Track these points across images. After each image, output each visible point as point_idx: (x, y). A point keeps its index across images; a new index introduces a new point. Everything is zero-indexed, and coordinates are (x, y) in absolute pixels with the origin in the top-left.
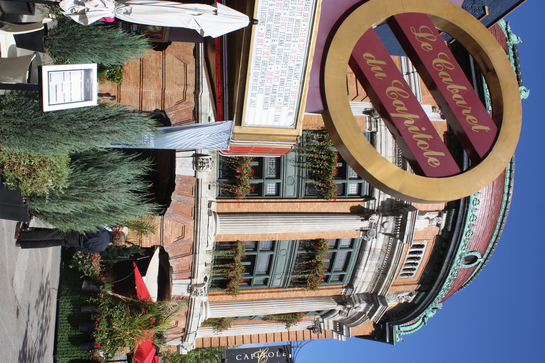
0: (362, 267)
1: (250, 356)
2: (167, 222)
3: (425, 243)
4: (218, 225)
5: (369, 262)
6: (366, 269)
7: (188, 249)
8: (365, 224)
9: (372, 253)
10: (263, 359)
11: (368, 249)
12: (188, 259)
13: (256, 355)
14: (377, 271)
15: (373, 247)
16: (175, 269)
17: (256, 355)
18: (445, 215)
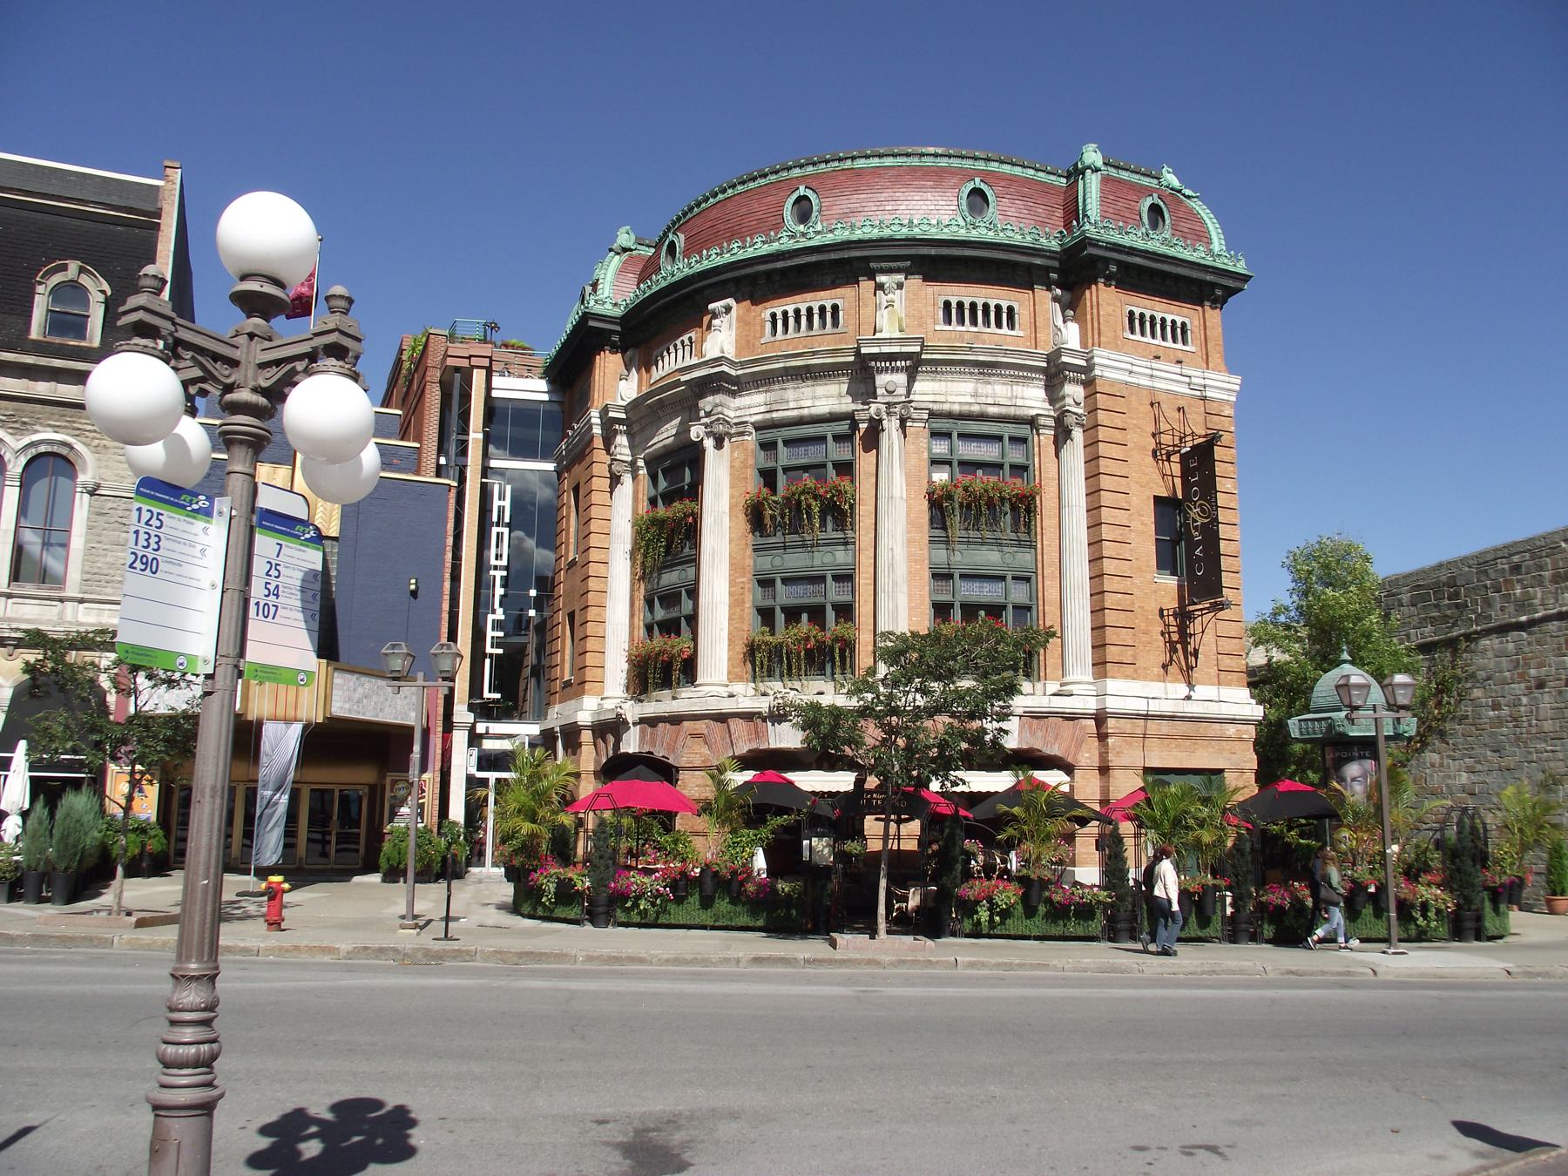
0: (805, 412)
1: (1198, 543)
2: (683, 762)
3: (767, 315)
4: (709, 680)
5: (792, 405)
6: (809, 403)
7: (717, 727)
8: (709, 443)
9: (775, 407)
10: (1203, 511)
11: (768, 416)
12: (737, 726)
13: (1196, 528)
14: (809, 383)
15: (763, 409)
16: (754, 746)
17: (1196, 528)
18: (711, 306)
